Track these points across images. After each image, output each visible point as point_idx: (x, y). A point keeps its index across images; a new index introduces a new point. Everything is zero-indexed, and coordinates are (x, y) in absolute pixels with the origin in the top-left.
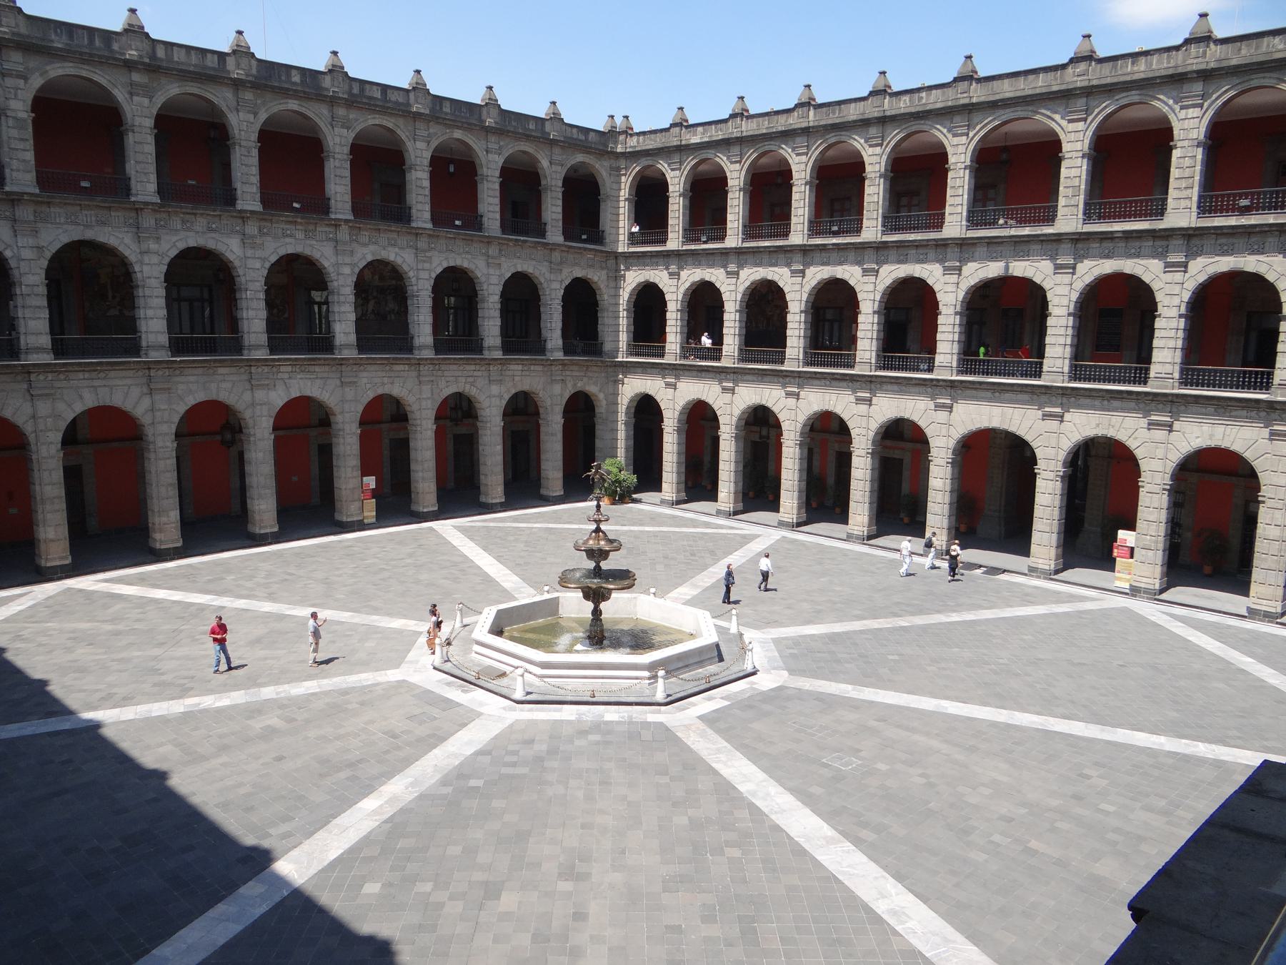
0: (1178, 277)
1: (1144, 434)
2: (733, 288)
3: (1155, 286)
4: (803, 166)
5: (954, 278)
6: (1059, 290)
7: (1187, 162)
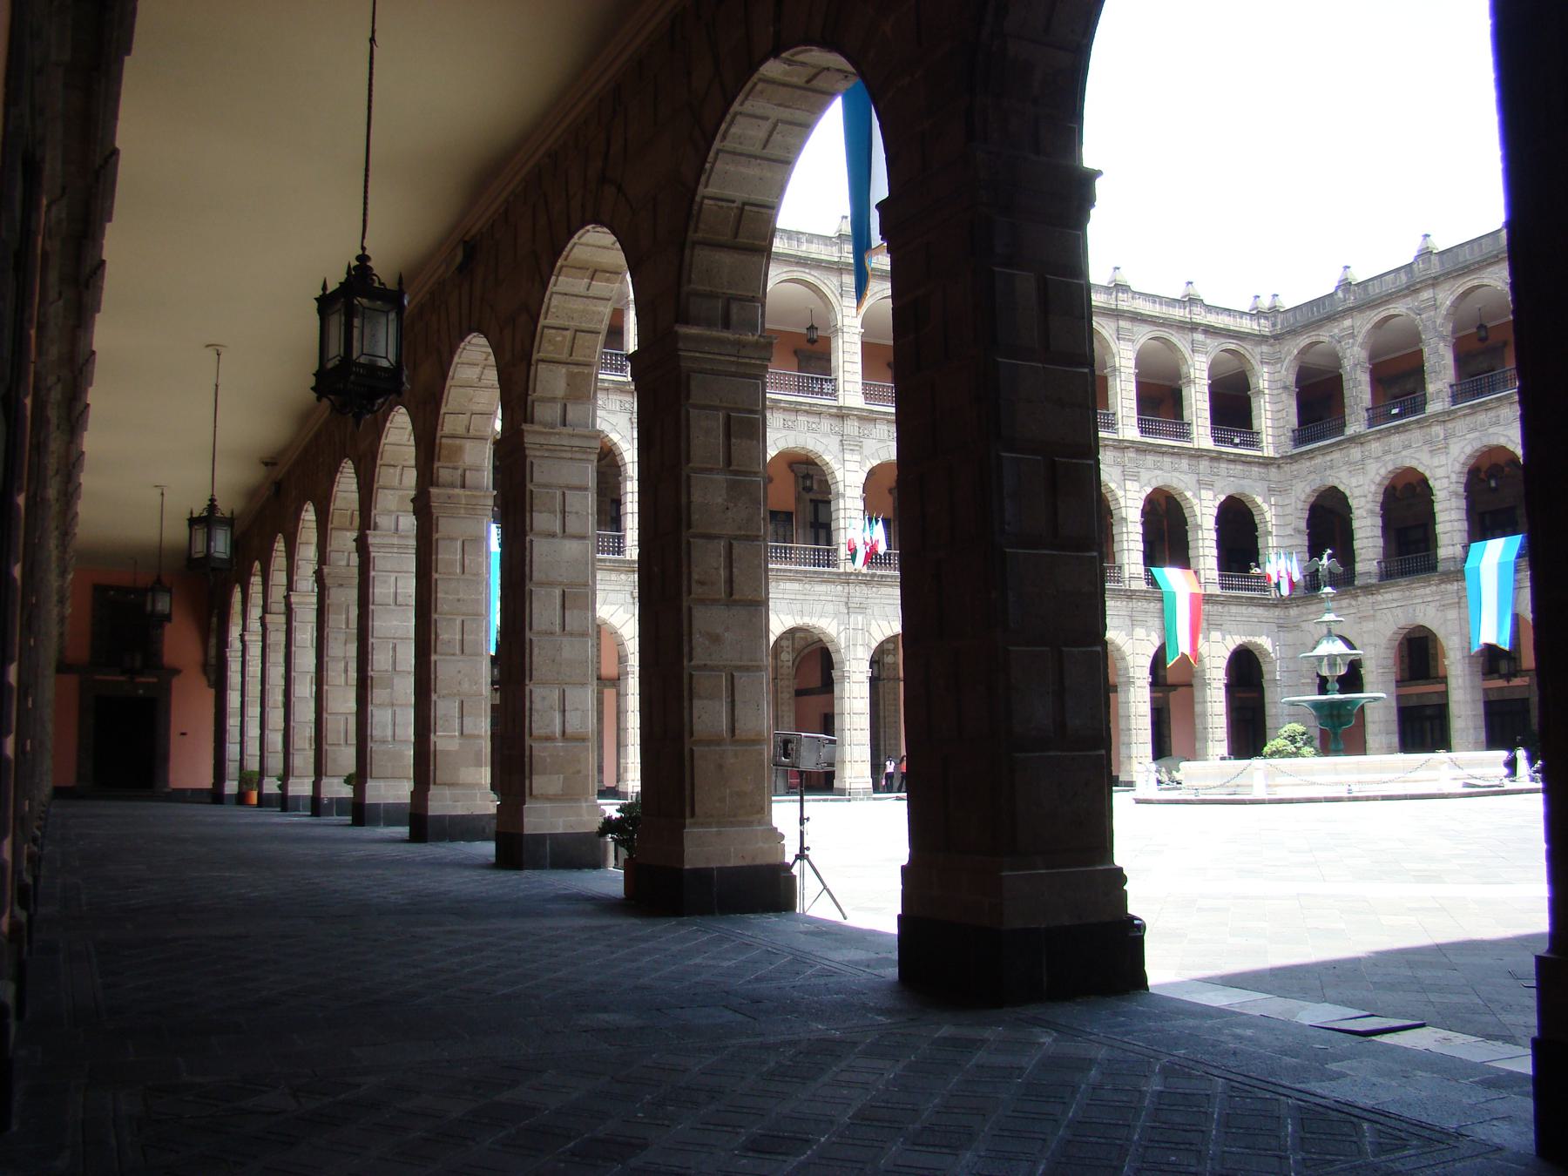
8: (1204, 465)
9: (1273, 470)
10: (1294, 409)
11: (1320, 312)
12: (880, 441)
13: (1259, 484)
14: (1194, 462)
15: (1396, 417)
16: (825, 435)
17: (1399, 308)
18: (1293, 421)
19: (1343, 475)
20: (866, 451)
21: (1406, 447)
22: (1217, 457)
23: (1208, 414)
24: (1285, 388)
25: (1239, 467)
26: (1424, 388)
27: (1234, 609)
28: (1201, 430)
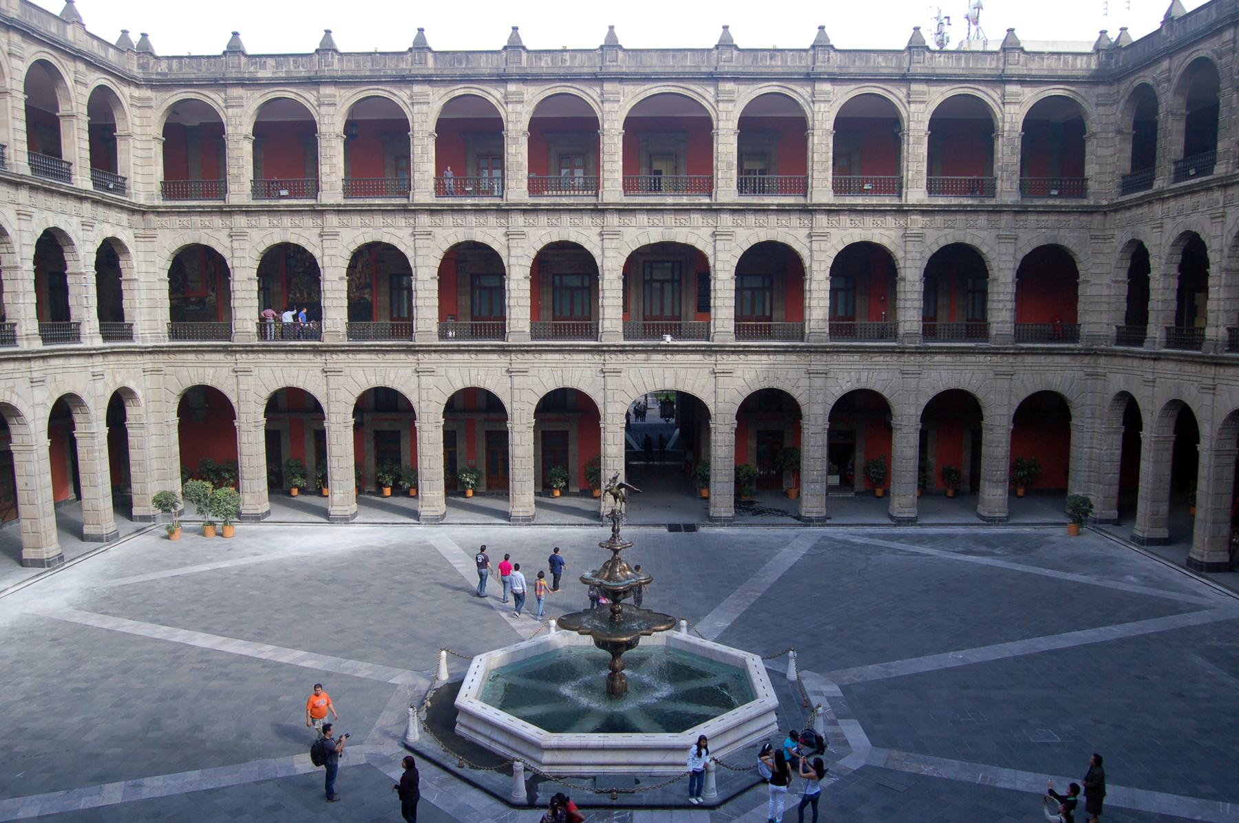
1: (804, 383)
8: (1005, 220)
9: (1098, 218)
10: (1128, 153)
11: (1151, 50)
12: (640, 228)
14: (994, 217)
15: (1196, 176)
17: (1205, 50)
18: (1127, 167)
19: (1147, 229)
20: (626, 238)
21: (1195, 210)
24: (1119, 132)
25: (1053, 218)
26: (1215, 147)
27: (1029, 360)
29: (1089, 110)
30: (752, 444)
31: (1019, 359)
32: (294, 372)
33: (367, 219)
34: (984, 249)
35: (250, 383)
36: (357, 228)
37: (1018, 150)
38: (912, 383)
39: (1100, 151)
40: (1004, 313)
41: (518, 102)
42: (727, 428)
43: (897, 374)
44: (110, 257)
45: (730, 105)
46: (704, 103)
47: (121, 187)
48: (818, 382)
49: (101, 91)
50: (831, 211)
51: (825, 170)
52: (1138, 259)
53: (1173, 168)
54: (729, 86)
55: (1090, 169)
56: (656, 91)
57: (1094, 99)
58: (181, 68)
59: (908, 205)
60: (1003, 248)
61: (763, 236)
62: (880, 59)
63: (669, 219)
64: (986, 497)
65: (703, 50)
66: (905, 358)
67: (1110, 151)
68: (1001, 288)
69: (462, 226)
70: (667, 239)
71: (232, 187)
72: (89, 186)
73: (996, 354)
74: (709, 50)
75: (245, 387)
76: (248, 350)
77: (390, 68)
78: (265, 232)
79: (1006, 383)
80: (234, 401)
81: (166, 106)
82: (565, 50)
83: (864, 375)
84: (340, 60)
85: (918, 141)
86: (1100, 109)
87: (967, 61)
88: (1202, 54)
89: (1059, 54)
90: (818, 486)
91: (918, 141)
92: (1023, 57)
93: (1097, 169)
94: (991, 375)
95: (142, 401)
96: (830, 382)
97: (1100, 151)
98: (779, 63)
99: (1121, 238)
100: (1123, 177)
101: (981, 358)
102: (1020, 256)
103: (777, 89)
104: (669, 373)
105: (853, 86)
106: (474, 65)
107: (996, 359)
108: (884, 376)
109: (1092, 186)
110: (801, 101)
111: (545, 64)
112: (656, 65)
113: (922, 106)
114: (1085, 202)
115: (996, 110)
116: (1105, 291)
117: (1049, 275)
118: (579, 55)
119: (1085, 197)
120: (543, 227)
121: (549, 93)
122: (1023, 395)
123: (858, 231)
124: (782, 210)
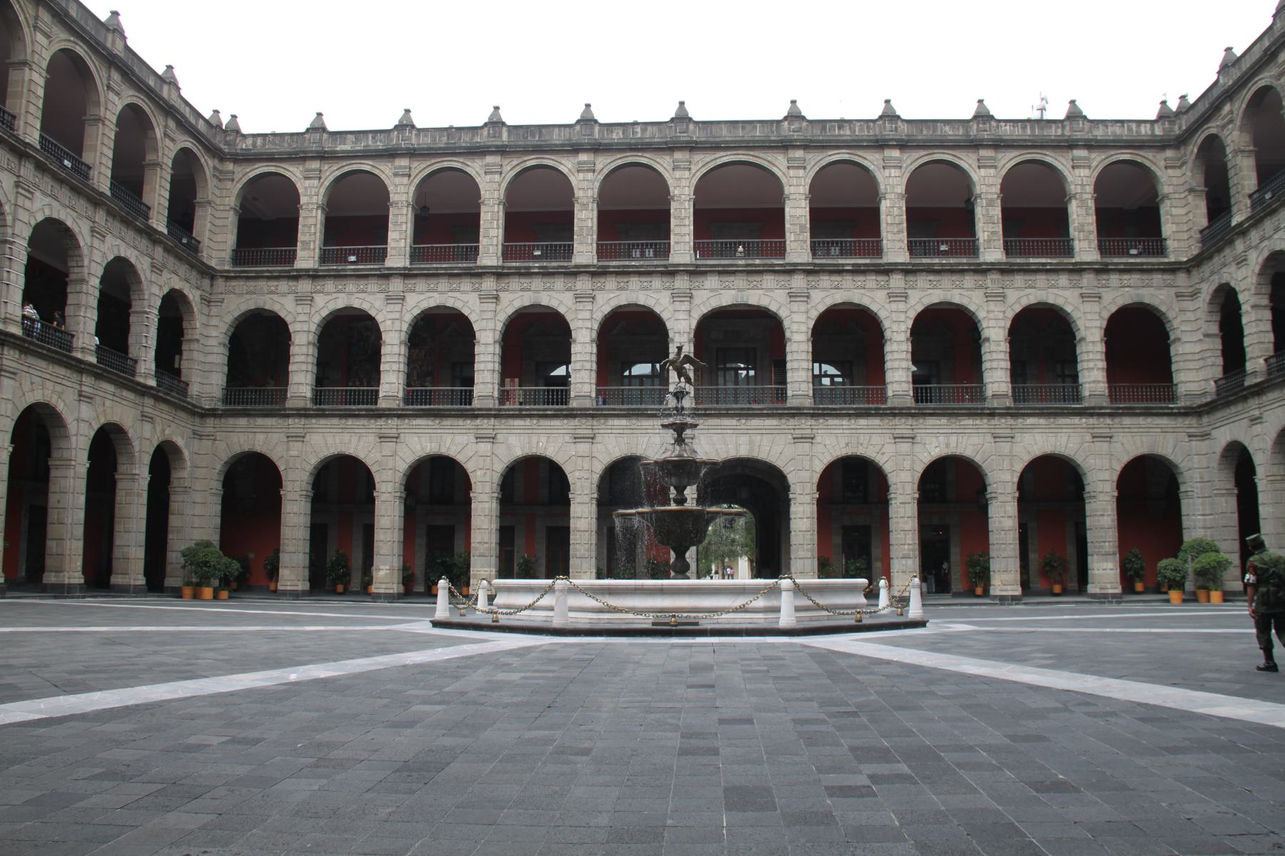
0: (902, 306)
1: (890, 448)
2: (397, 315)
3: (882, 315)
4: (495, 186)
5: (685, 306)
6: (796, 317)
7: (896, 211)
8: (1088, 279)
12: (711, 290)
13: (1164, 291)
14: (1076, 277)
16: (657, 290)
18: (1204, 222)
20: (697, 301)
22: (1102, 270)
23: (1093, 228)
24: (1191, 190)
28: (1084, 245)
29: (1159, 173)
30: (837, 540)
31: (1117, 420)
32: (346, 437)
33: (432, 282)
34: (1068, 309)
35: (300, 448)
36: (422, 293)
37: (1093, 211)
38: (1005, 447)
39: (1174, 211)
40: (1095, 372)
41: (588, 171)
42: (808, 499)
43: (989, 438)
44: (164, 459)
45: (801, 172)
46: (774, 170)
47: (183, 389)
48: (905, 447)
49: (185, 152)
50: (908, 271)
51: (900, 232)
52: (1227, 306)
53: (1249, 202)
54: (799, 154)
55: (1167, 229)
56: (726, 159)
57: (1162, 164)
58: (264, 145)
59: (987, 264)
60: (1092, 307)
61: (838, 297)
62: (947, 128)
63: (739, 281)
64: (1096, 572)
65: (772, 122)
66: (996, 421)
67: (1183, 211)
68: (1090, 347)
69: (530, 290)
70: (740, 301)
71: (300, 253)
72: (152, 383)
73: (1092, 415)
74: (778, 122)
75: (295, 453)
76: (302, 413)
77: (465, 140)
78: (329, 297)
79: (1105, 445)
80: (281, 468)
81: (245, 180)
82: (635, 124)
83: (953, 438)
84: (418, 136)
85: (990, 203)
86: (1170, 172)
87: (1032, 129)
88: (1261, 84)
89: (1122, 122)
90: (910, 562)
91: (990, 203)
92: (1087, 125)
93: (1174, 228)
94: (1088, 438)
95: (189, 464)
96: (917, 448)
97: (1174, 211)
98: (848, 133)
99: (1207, 290)
100: (1201, 232)
101: (1076, 420)
102: (1106, 315)
103: (846, 157)
104: (744, 439)
105: (922, 153)
106: (547, 138)
107: (1092, 421)
108: (975, 439)
109: (1171, 244)
110: (872, 168)
111: (617, 136)
112: (725, 135)
113: (992, 171)
114: (1166, 260)
115: (1066, 173)
116: (1198, 348)
117: (1139, 346)
118: (649, 128)
119: (1166, 257)
120: (611, 291)
121: (620, 162)
122: (1126, 459)
123: (937, 292)
124: (857, 271)
